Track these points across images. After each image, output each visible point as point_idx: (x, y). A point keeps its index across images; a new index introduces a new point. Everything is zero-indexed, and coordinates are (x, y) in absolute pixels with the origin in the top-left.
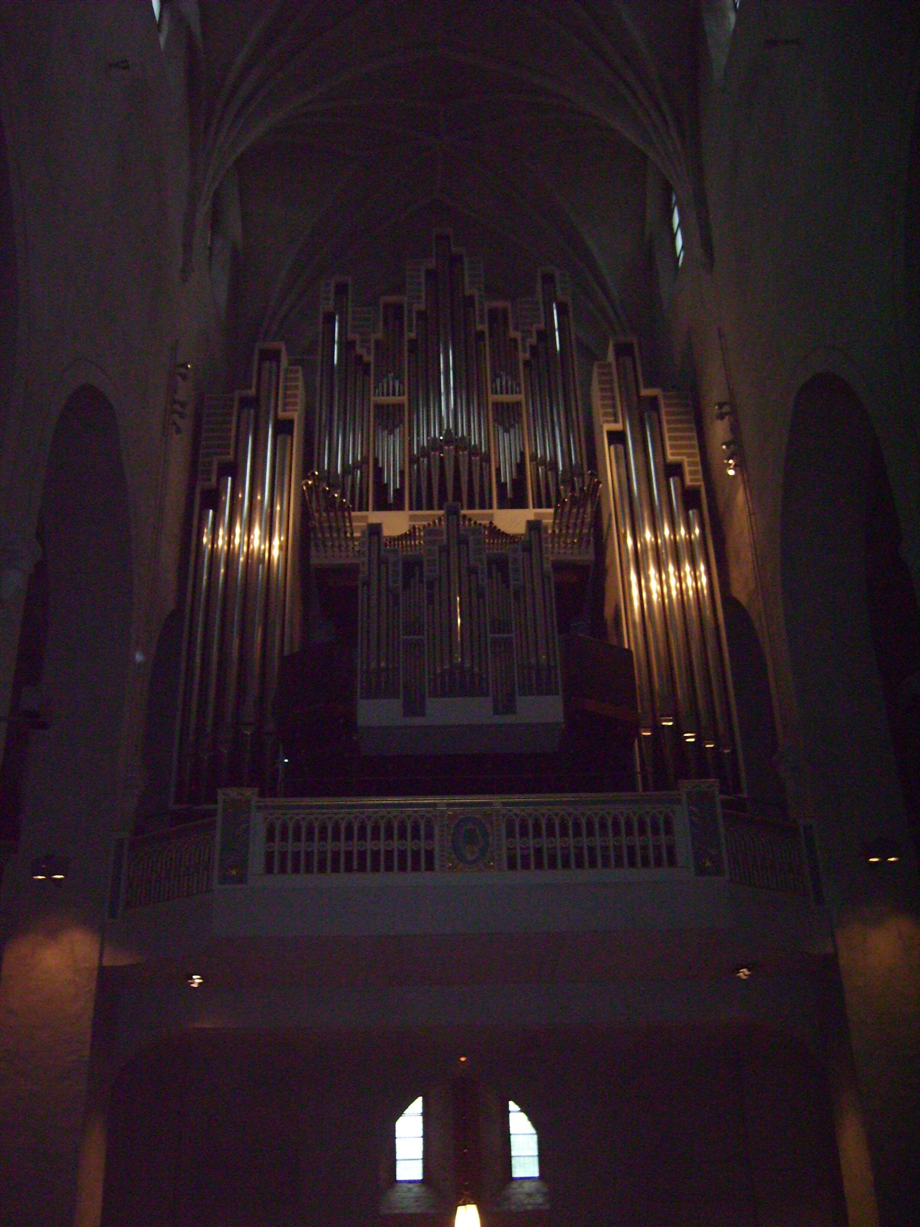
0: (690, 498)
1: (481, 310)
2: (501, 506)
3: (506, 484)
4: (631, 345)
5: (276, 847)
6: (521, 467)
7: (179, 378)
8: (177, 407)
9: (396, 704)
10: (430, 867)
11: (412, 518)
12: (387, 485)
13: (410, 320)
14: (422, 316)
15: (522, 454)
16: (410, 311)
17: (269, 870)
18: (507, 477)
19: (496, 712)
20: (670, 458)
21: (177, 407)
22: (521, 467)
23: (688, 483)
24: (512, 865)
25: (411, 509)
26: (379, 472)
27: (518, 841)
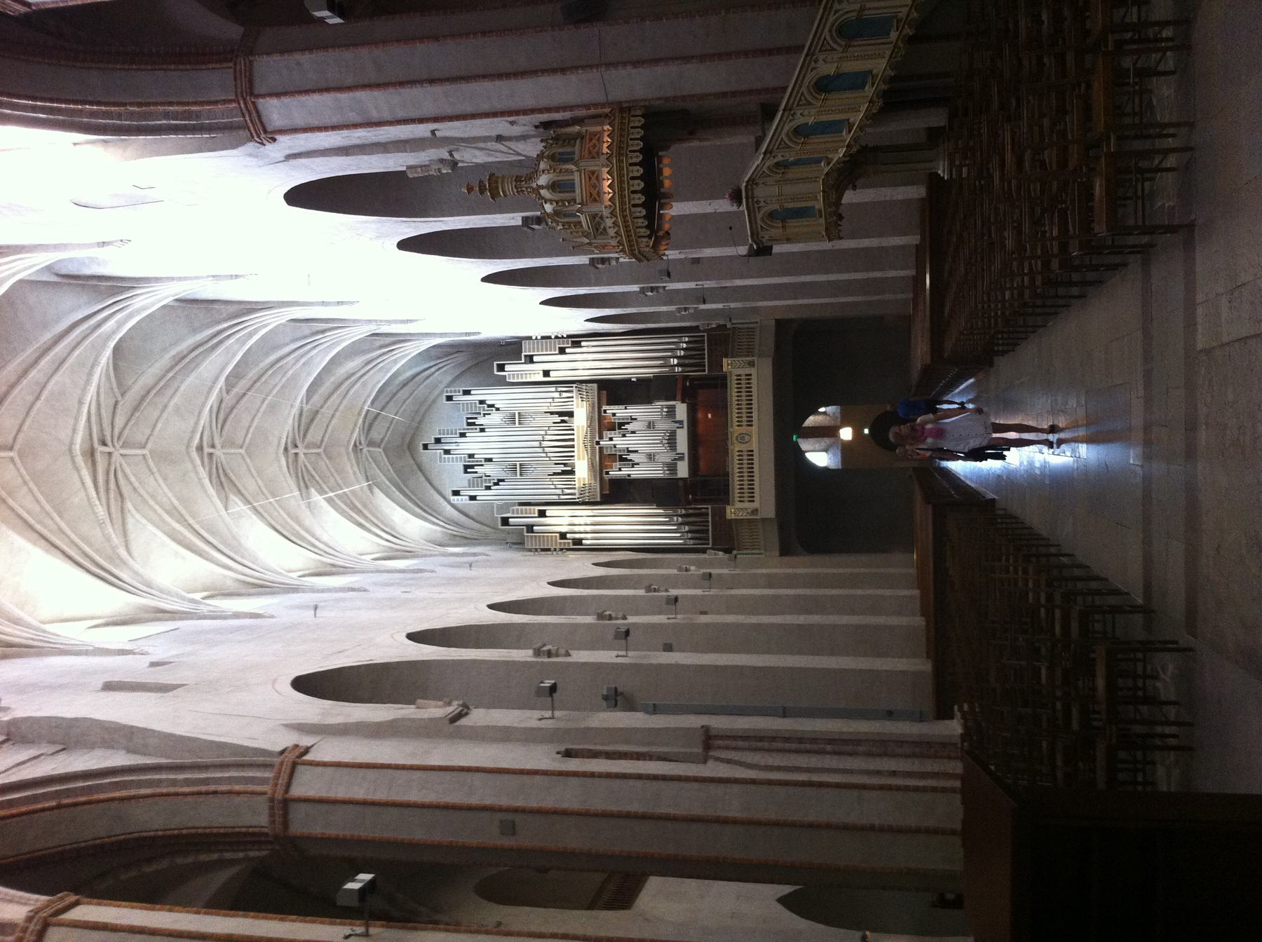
6: (552, 413)
9: (679, 463)
18: (558, 419)
22: (552, 413)
26: (555, 474)
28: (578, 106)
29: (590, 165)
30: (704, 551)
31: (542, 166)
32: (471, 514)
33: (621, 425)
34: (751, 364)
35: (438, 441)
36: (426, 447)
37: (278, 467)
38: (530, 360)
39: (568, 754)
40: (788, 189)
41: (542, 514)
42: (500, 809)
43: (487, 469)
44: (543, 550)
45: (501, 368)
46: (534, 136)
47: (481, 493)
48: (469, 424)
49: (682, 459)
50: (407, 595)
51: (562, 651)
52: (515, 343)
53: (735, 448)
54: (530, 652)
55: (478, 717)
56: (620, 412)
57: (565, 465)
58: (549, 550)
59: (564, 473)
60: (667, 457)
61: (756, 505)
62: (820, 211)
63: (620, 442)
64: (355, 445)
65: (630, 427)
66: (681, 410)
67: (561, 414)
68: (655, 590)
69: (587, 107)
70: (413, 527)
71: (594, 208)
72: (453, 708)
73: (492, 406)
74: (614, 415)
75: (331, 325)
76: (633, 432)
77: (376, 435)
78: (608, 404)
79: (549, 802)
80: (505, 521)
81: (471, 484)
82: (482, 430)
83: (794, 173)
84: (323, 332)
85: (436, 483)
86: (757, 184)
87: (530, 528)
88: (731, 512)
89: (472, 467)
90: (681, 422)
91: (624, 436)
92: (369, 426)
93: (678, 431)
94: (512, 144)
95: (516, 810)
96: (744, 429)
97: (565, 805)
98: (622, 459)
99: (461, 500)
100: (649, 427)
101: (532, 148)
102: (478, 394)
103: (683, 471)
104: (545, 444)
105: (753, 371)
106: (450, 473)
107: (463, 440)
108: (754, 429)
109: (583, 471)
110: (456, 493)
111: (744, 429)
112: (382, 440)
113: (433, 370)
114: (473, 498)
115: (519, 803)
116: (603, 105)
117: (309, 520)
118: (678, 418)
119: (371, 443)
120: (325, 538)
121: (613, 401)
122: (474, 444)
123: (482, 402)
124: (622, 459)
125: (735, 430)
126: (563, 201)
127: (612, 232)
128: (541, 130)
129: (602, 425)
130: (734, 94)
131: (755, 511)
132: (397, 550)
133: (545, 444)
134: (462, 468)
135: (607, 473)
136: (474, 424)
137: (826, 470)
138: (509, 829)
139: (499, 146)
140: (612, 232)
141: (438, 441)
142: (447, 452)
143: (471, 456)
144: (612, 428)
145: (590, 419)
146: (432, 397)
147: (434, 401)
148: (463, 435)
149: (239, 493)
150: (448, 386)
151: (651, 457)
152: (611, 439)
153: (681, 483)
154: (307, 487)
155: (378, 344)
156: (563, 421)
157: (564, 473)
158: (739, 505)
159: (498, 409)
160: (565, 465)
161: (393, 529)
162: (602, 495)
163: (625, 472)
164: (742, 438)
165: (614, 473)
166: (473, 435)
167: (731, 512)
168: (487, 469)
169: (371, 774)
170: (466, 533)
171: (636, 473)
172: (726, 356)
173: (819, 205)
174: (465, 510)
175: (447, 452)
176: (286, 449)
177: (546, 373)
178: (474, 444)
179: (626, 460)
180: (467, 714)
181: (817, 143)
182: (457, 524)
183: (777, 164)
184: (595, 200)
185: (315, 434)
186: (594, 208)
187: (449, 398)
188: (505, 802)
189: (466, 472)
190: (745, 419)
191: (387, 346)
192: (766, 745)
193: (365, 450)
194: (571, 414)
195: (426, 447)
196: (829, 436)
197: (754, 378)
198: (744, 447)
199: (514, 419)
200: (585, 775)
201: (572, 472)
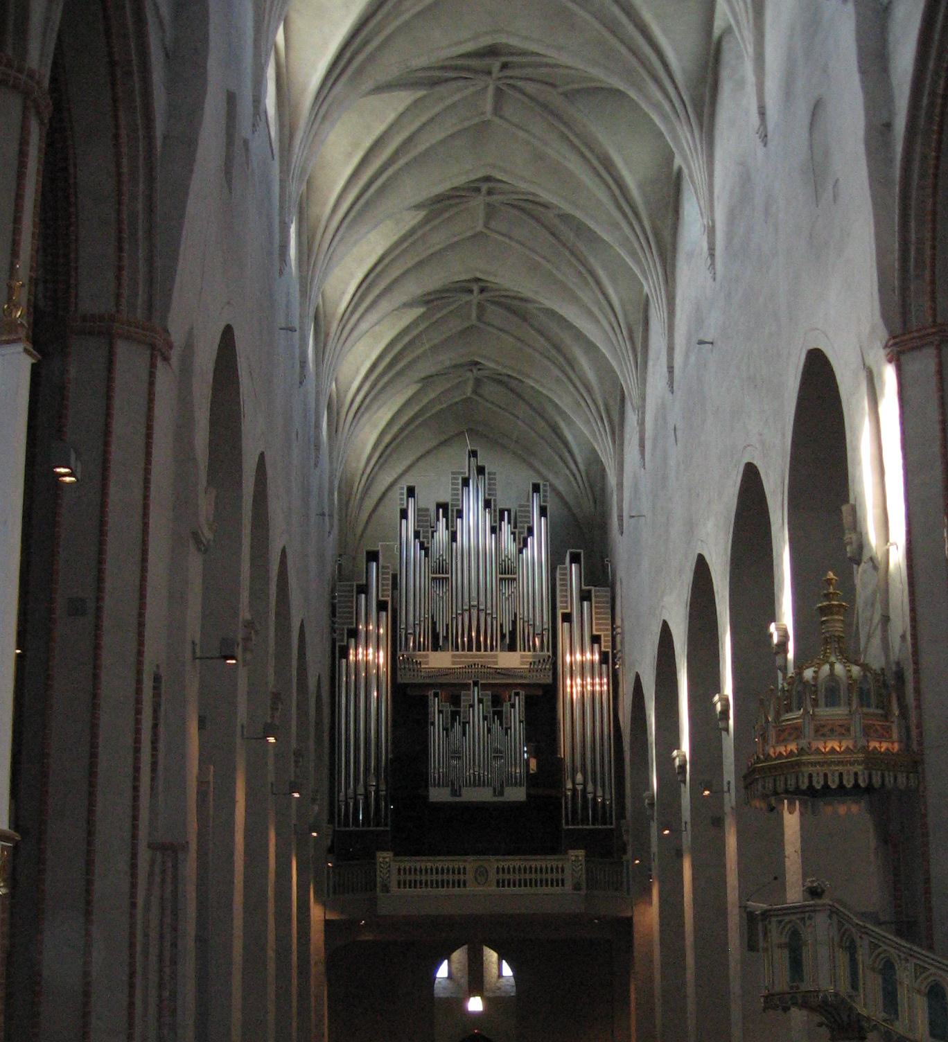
1: (495, 511)
2: (502, 650)
4: (580, 554)
6: (514, 623)
9: (448, 790)
11: (453, 656)
12: (438, 634)
13: (452, 516)
16: (452, 511)
18: (506, 630)
19: (495, 795)
20: (595, 633)
22: (514, 623)
23: (603, 649)
25: (452, 651)
26: (434, 624)
28: (920, 716)
29: (856, 728)
30: (331, 821)
31: (855, 670)
32: (381, 509)
33: (499, 714)
34: (577, 887)
35: (481, 471)
36: (473, 454)
37: (455, 270)
38: (585, 596)
39: (157, 679)
40: (824, 952)
41: (382, 606)
42: (99, 599)
43: (442, 534)
44: (333, 607)
45: (575, 559)
46: (887, 662)
47: (409, 526)
48: (502, 512)
49: (455, 793)
50: (294, 436)
51: (249, 656)
52: (605, 572)
53: (470, 863)
54: (248, 616)
55: (195, 564)
56: (516, 714)
57: (446, 638)
58: (333, 614)
59: (435, 636)
61: (394, 888)
62: (798, 988)
63: (476, 714)
64: (477, 363)
65: (496, 726)
66: (517, 794)
67: (513, 633)
68: (296, 762)
69: (919, 726)
70: (367, 435)
71: (809, 730)
72: (207, 535)
73: (525, 545)
74: (513, 706)
75: (639, 349)
76: (489, 731)
77: (489, 389)
78: (527, 697)
79: (106, 659)
80: (373, 556)
81: (421, 513)
82: (493, 530)
83: (843, 958)
84: (631, 339)
85: (421, 464)
86: (830, 917)
87: (364, 589)
88: (384, 857)
89: (445, 515)
90: (501, 794)
91: (485, 718)
92: (499, 380)
94: (878, 633)
95: (98, 617)
96: (493, 876)
97: (104, 678)
98: (455, 714)
99: (398, 497)
100: (496, 751)
101: (875, 658)
102: (540, 526)
103: (438, 795)
104: (474, 612)
105: (568, 887)
106: (435, 486)
107: (481, 504)
108: (494, 888)
109: (440, 660)
110: (411, 492)
111: (493, 876)
112: (480, 396)
113: (573, 466)
114: (404, 514)
115: (106, 624)
116: (920, 744)
117: (385, 306)
119: (478, 382)
120: (364, 326)
121: (530, 703)
122: (474, 517)
123: (530, 531)
124: (455, 714)
125: (494, 863)
126: (815, 692)
127: (782, 749)
128: (894, 668)
129: (498, 691)
130: (927, 891)
131: (386, 888)
133: (474, 612)
134: (442, 500)
135: (436, 695)
136: (502, 519)
137: (433, 978)
138: (77, 608)
139: (877, 618)
140: (782, 749)
141: (481, 471)
142: (466, 482)
143: (460, 514)
144: (497, 701)
145: (506, 672)
146: (537, 464)
147: (531, 466)
148: (487, 504)
149: (426, 221)
150: (554, 489)
151: (456, 754)
152: (480, 701)
154: (427, 302)
155: (611, 403)
156: (503, 636)
157: (435, 636)
158: (394, 867)
159: (521, 551)
160: (446, 638)
161: (367, 408)
162: (406, 685)
163: (437, 719)
164: (481, 873)
165: (435, 705)
166: (486, 520)
167: (384, 857)
168: (442, 534)
169: (140, 441)
170: (354, 503)
171: (436, 733)
172: (586, 856)
173: (804, 987)
174: (386, 500)
176: (478, 280)
177: (567, 618)
178: (474, 517)
179: (453, 720)
180: (199, 550)
181: (872, 983)
182: (367, 488)
183: (853, 942)
184: (817, 731)
185: (495, 315)
186: (809, 730)
187: (536, 488)
188: (108, 603)
189: (439, 506)
190: (507, 877)
191: (609, 416)
192: (168, 920)
193: (469, 374)
194: (512, 647)
195: (473, 454)
196: (470, 982)
197: (558, 890)
198: (469, 876)
199: (507, 573)
200: (138, 701)
201: (436, 647)
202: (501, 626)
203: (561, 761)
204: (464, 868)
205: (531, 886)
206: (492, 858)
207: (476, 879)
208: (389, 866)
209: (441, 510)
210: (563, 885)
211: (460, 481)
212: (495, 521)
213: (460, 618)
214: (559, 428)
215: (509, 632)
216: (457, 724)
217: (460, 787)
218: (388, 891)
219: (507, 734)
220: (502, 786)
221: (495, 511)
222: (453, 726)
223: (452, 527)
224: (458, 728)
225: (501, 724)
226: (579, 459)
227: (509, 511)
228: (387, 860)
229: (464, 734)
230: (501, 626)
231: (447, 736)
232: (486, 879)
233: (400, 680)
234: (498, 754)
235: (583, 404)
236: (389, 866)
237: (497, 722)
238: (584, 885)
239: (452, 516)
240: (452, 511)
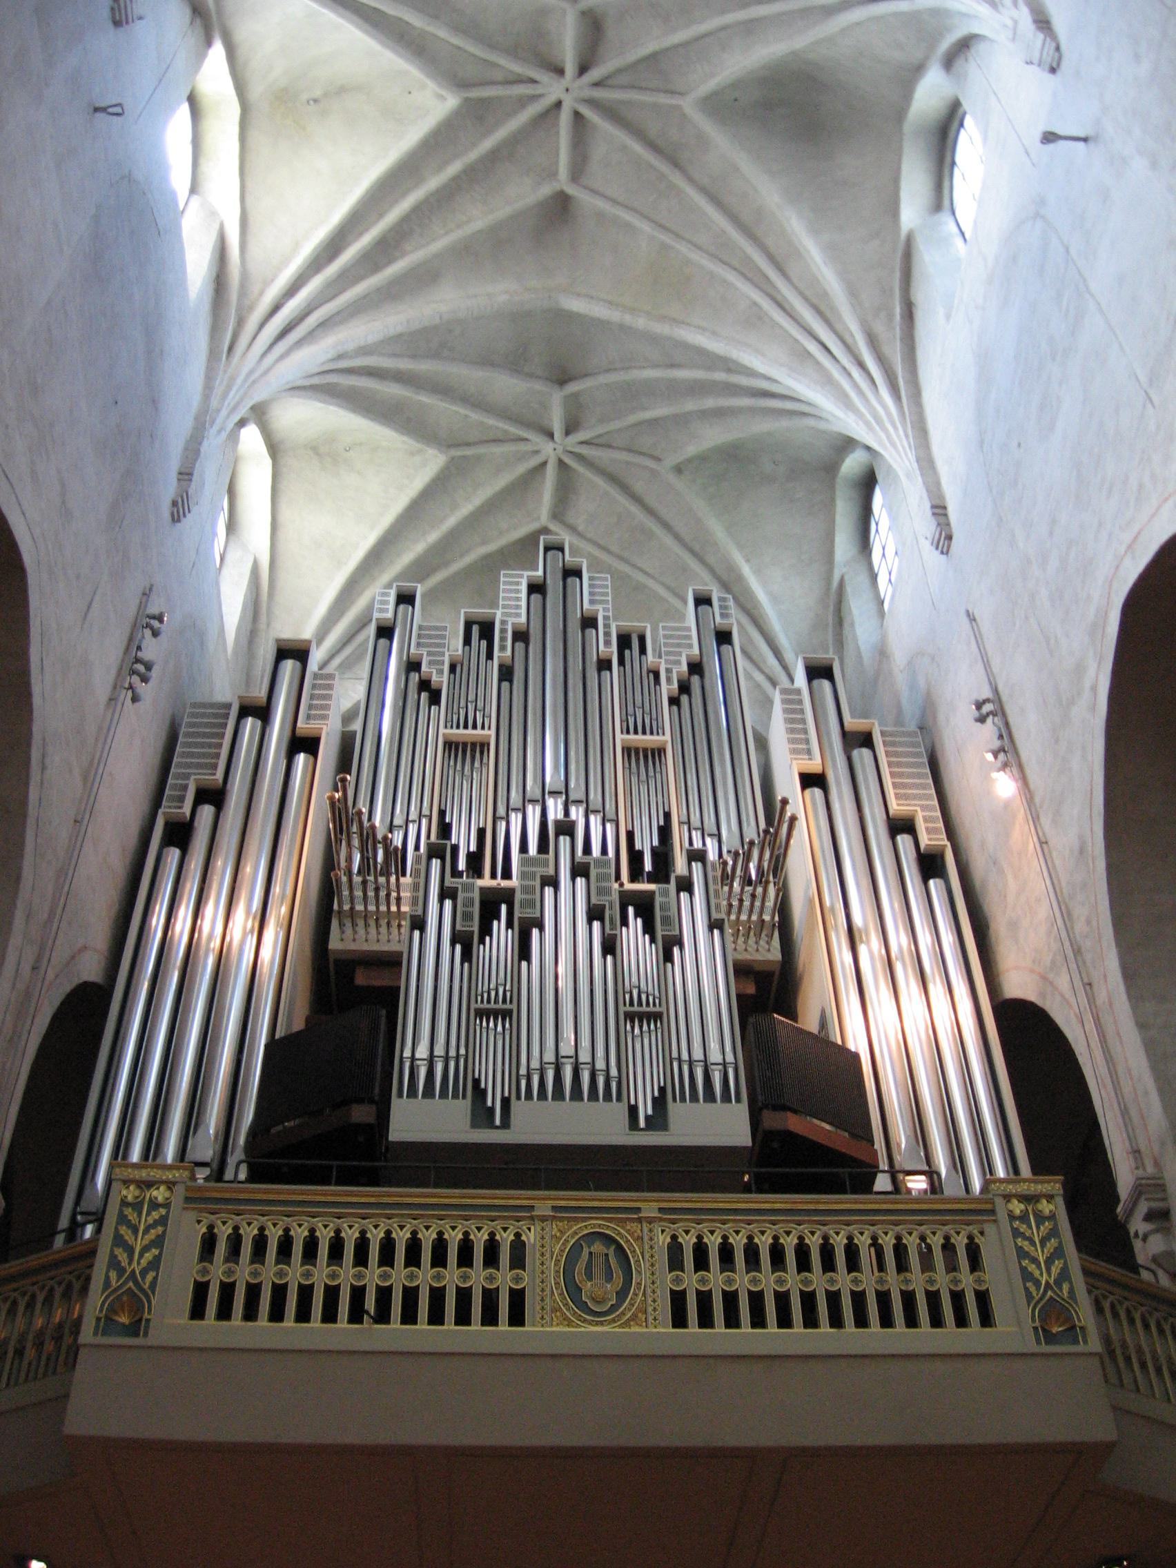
0: (930, 865)
1: (607, 634)
3: (641, 853)
5: (218, 1271)
6: (665, 832)
7: (148, 632)
8: (141, 668)
9: (462, 1108)
10: (517, 1318)
13: (503, 639)
14: (521, 636)
15: (667, 816)
16: (503, 631)
17: (198, 1311)
18: (646, 842)
20: (895, 807)
21: (141, 668)
22: (665, 832)
24: (679, 1320)
27: (691, 1281)
34: (1053, 1320)
49: (481, 1115)
60: (492, 1074)
61: (169, 1317)
65: (633, 935)
76: (610, 947)
90: (659, 1120)
91: (595, 914)
93: (621, 1110)
96: (654, 1280)
105: (1014, 1328)
108: (657, 1331)
110: (405, 599)
118: (675, 1109)
131: (130, 1312)
132: (240, 322)
152: (579, 870)
153: (362, 1114)
162: (352, 963)
175: (536, 588)
197: (974, 1337)
198: (542, 1277)
202: (630, 836)
203: (856, 1057)
204: (518, 1246)
205: (836, 1321)
206: (650, 1204)
207: (574, 1291)
208: (163, 1221)
209: (475, 629)
210: (986, 1319)
211: (524, 588)
212: (608, 643)
213: (516, 820)
214: (740, 578)
215: (653, 849)
216: (499, 926)
217: (506, 1102)
218: (135, 1328)
219: (668, 957)
220: (660, 1102)
221: (607, 634)
222: (486, 930)
223: (503, 648)
224: (502, 936)
225: (649, 929)
226: (784, 641)
227: (642, 639)
228: (160, 1194)
229: (524, 952)
230: (630, 836)
231: (467, 956)
232: (622, 1294)
233: (337, 942)
234: (643, 1014)
235: (813, 347)
236: (163, 1221)
237: (636, 924)
238: (1085, 1314)
239: (503, 639)
240: (503, 631)
